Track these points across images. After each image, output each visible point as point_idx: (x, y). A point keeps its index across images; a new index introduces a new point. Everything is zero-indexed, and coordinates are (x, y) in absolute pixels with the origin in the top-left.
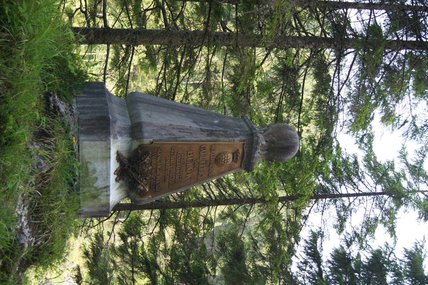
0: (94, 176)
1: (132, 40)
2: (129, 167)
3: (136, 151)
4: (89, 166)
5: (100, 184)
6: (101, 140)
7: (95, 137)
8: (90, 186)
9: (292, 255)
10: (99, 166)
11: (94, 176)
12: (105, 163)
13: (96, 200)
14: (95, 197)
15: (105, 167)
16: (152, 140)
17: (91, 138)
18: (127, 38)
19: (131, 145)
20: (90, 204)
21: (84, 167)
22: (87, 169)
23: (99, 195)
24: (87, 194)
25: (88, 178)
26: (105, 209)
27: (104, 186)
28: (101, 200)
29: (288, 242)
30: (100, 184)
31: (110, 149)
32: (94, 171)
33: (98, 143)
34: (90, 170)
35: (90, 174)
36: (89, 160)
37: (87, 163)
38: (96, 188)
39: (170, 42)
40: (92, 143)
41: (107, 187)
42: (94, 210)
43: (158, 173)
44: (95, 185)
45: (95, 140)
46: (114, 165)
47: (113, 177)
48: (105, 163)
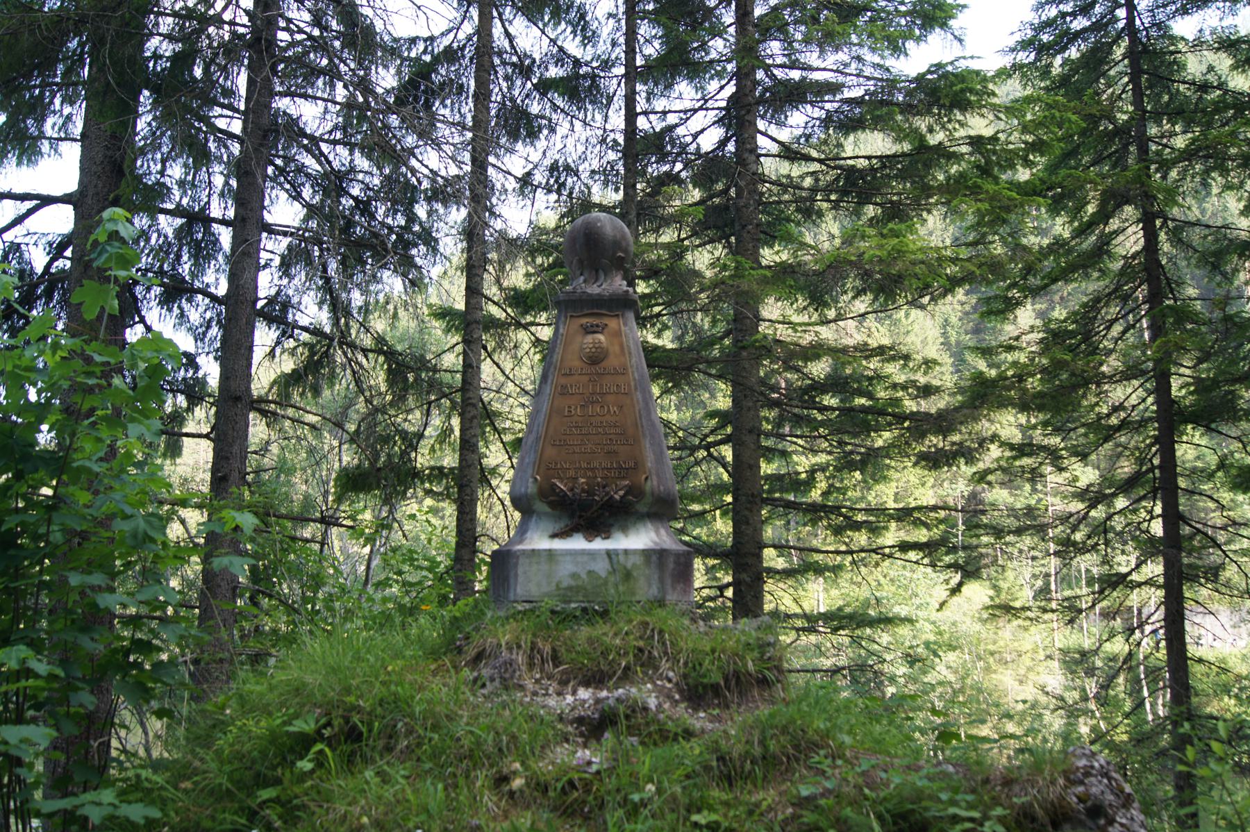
0: (584, 576)
1: (750, 502)
2: (580, 517)
3: (552, 505)
4: (565, 584)
5: (602, 567)
6: (516, 565)
7: (512, 574)
8: (606, 583)
9: (758, 162)
10: (565, 570)
11: (584, 576)
12: (560, 558)
13: (635, 574)
14: (628, 576)
15: (568, 558)
16: (531, 480)
17: (512, 581)
18: (747, 513)
19: (546, 514)
20: (642, 582)
21: (566, 594)
22: (570, 588)
23: (625, 568)
24: (621, 588)
25: (589, 587)
26: (654, 558)
27: (607, 560)
28: (634, 564)
29: (1180, 142)
30: (602, 567)
31: (533, 550)
32: (574, 576)
33: (520, 570)
34: (573, 583)
35: (580, 583)
36: (554, 584)
37: (558, 587)
38: (610, 573)
39: (750, 432)
40: (520, 579)
41: (609, 553)
42: (656, 576)
43: (596, 464)
44: (603, 574)
45: (516, 575)
46: (577, 543)
47: (599, 544)
48: (560, 558)
